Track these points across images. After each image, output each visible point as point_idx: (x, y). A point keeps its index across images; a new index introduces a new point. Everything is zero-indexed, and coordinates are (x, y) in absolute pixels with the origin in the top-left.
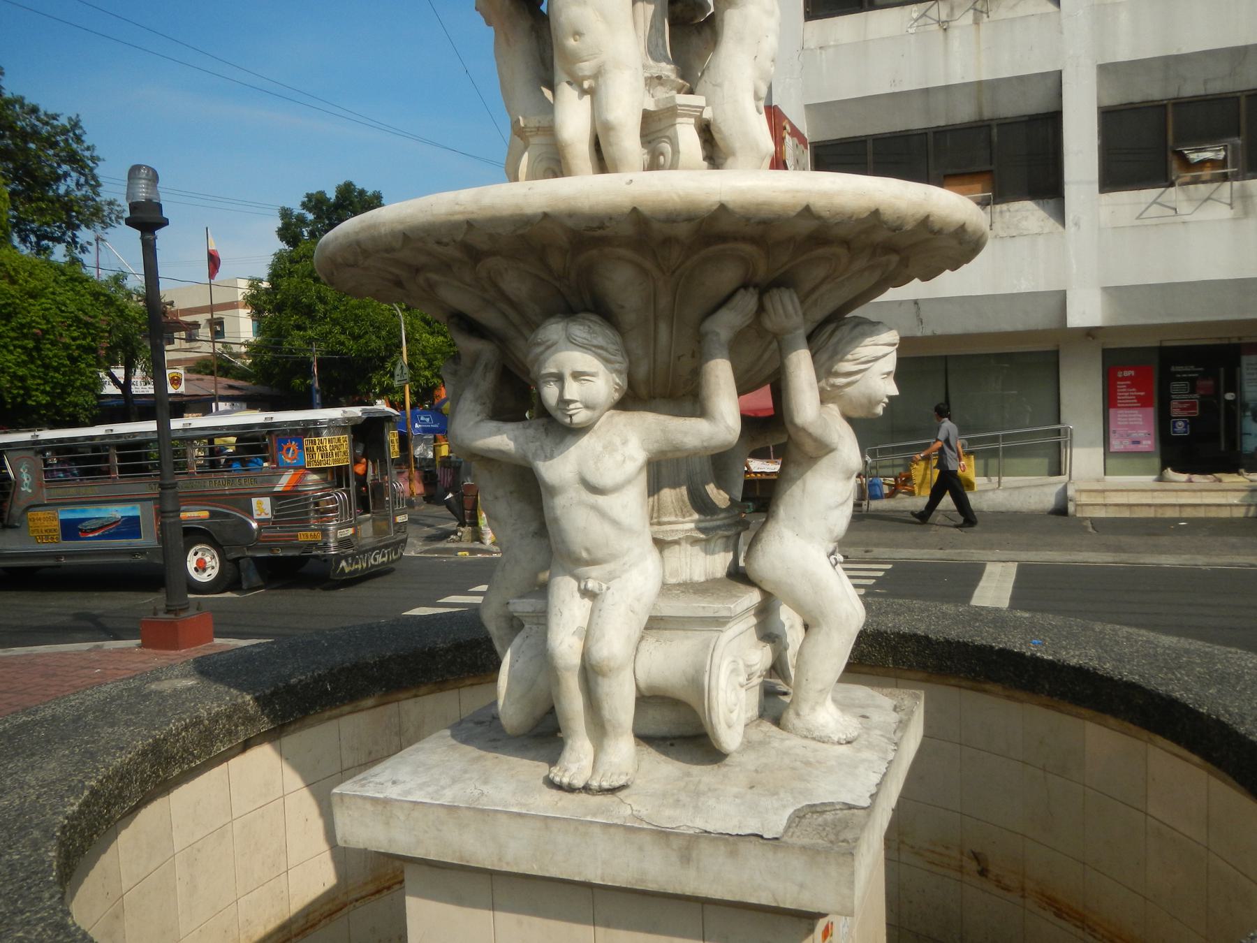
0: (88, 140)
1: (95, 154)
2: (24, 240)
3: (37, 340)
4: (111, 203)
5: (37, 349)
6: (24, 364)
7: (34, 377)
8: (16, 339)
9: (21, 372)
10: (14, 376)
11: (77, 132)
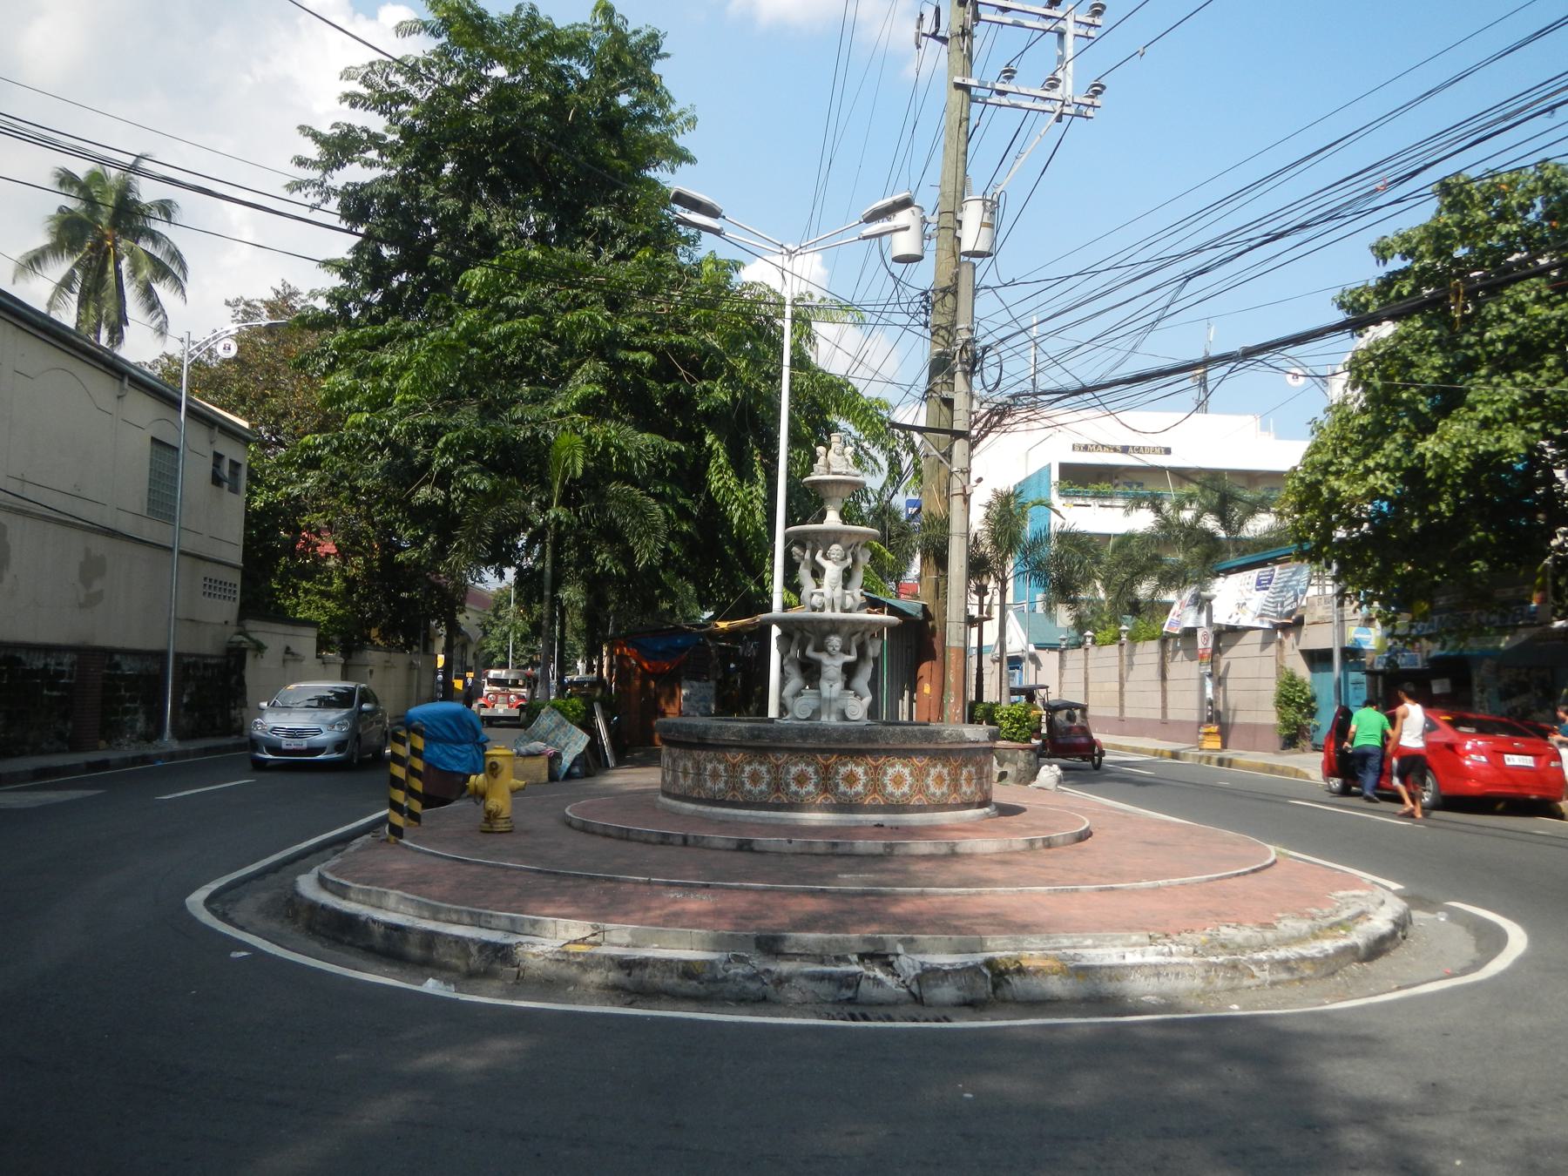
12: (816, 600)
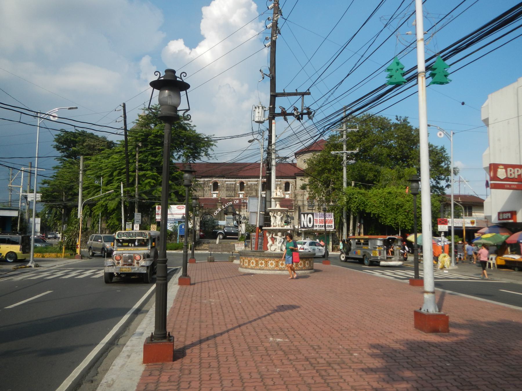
0: (447, 152)
1: (448, 156)
2: (434, 180)
3: (408, 213)
5: (408, 215)
6: (405, 219)
7: (408, 222)
9: (404, 221)
10: (402, 222)
12: (275, 224)
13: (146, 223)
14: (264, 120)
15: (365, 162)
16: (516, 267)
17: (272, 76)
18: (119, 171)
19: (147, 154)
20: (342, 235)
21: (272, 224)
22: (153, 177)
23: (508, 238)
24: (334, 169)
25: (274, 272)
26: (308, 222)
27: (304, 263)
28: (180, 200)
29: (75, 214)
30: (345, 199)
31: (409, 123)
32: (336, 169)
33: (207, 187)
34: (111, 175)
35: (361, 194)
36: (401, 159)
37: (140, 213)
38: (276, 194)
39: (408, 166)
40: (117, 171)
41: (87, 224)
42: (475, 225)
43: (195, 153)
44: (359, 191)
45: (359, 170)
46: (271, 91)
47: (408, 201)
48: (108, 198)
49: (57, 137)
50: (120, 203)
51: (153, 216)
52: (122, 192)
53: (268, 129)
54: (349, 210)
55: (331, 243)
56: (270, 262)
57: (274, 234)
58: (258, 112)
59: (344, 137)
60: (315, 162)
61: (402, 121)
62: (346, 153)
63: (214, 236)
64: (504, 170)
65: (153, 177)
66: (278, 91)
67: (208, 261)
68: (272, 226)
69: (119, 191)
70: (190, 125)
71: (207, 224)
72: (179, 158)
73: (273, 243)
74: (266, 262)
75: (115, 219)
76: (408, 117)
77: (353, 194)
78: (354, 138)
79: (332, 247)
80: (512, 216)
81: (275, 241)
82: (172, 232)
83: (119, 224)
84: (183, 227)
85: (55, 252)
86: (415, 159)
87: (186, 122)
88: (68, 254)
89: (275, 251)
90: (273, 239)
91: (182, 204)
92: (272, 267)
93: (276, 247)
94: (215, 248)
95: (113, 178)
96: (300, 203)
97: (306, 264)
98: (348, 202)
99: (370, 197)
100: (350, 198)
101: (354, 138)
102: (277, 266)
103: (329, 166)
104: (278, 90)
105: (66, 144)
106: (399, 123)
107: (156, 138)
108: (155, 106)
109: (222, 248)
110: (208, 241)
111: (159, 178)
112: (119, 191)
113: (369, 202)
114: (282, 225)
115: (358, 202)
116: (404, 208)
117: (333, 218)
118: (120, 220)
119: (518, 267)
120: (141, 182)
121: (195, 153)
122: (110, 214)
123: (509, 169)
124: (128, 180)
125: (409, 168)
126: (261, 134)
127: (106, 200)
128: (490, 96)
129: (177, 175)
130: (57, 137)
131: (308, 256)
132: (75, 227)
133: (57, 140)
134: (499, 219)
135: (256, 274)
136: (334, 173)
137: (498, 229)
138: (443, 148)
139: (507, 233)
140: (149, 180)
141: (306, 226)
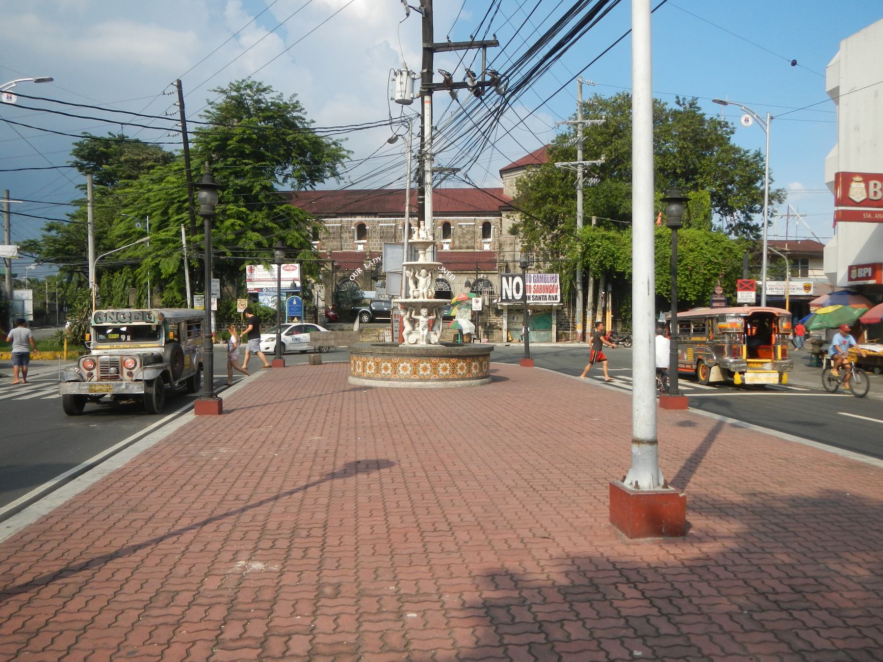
0: (767, 161)
2: (742, 212)
3: (691, 272)
4: (779, 190)
5: (691, 275)
6: (685, 282)
7: (690, 288)
8: (683, 270)
11: (762, 156)
12: (416, 294)
13: (231, 295)
14: (413, 98)
15: (617, 182)
16: (877, 366)
17: (425, 10)
18: (178, 204)
19: (226, 173)
20: (574, 312)
21: (411, 292)
22: (239, 216)
23: (864, 313)
24: (563, 195)
25: (410, 383)
26: (515, 291)
27: (469, 365)
28: (291, 255)
29: (108, 282)
30: (579, 248)
31: (699, 108)
32: (567, 196)
33: (346, 232)
34: (165, 213)
35: (608, 239)
36: (683, 175)
37: (218, 280)
38: (419, 235)
39: (695, 187)
40: (176, 205)
41: (128, 300)
42: (811, 292)
43: (316, 171)
44: (605, 233)
45: (606, 196)
46: (425, 41)
47: (692, 251)
48: (159, 253)
49: (77, 147)
50: (182, 262)
51: (242, 284)
52: (184, 242)
53: (419, 115)
54: (586, 269)
55: (554, 327)
56: (401, 365)
57: (414, 312)
58: (401, 83)
59: (580, 134)
60: (530, 185)
61: (688, 106)
62: (583, 166)
63: (351, 316)
64: (863, 185)
65: (239, 216)
66: (436, 40)
67: (310, 364)
68: (412, 297)
69: (178, 241)
70: (304, 119)
71: (342, 297)
72: (285, 180)
73: (414, 329)
74: (395, 365)
75: (175, 290)
76: (697, 99)
77: (594, 240)
78: (599, 139)
79: (557, 333)
80: (874, 272)
81: (416, 325)
82: (276, 312)
83: (183, 299)
84: (295, 303)
85: (51, 350)
86: (708, 175)
87: (295, 114)
88: (75, 353)
89: (416, 343)
90: (413, 322)
91: (293, 262)
92: (405, 374)
93: (418, 337)
94: (323, 340)
95: (169, 218)
96: (508, 258)
97: (473, 368)
98: (584, 254)
99: (625, 245)
100: (588, 247)
101: (599, 139)
102: (415, 373)
103: (554, 191)
104: (439, 38)
105: (93, 160)
106: (681, 109)
107: (242, 144)
108: (236, 84)
109: (335, 339)
110: (341, 326)
111: (250, 217)
112: (178, 241)
113: (621, 254)
114: (430, 294)
115: (602, 254)
116: (684, 262)
117: (558, 283)
118: (183, 291)
119: (880, 367)
120: (218, 224)
121: (314, 173)
122: (166, 281)
123: (872, 183)
124: (193, 220)
125: (697, 191)
126: (407, 124)
127: (158, 256)
128: (843, 44)
129: (281, 210)
130: (77, 147)
131: (475, 353)
132: (85, 306)
133: (77, 153)
134: (850, 279)
135: (376, 388)
136: (563, 203)
137: (848, 297)
138: (758, 155)
139: (864, 305)
140: (232, 220)
141: (510, 298)
